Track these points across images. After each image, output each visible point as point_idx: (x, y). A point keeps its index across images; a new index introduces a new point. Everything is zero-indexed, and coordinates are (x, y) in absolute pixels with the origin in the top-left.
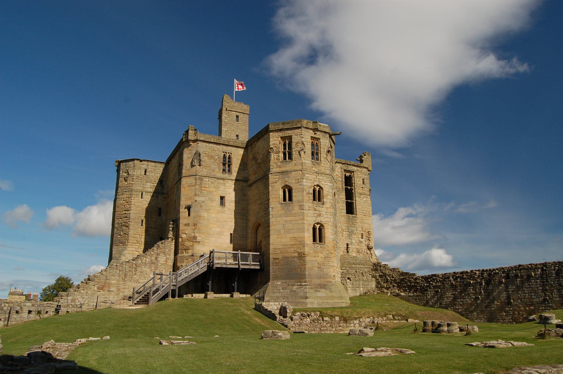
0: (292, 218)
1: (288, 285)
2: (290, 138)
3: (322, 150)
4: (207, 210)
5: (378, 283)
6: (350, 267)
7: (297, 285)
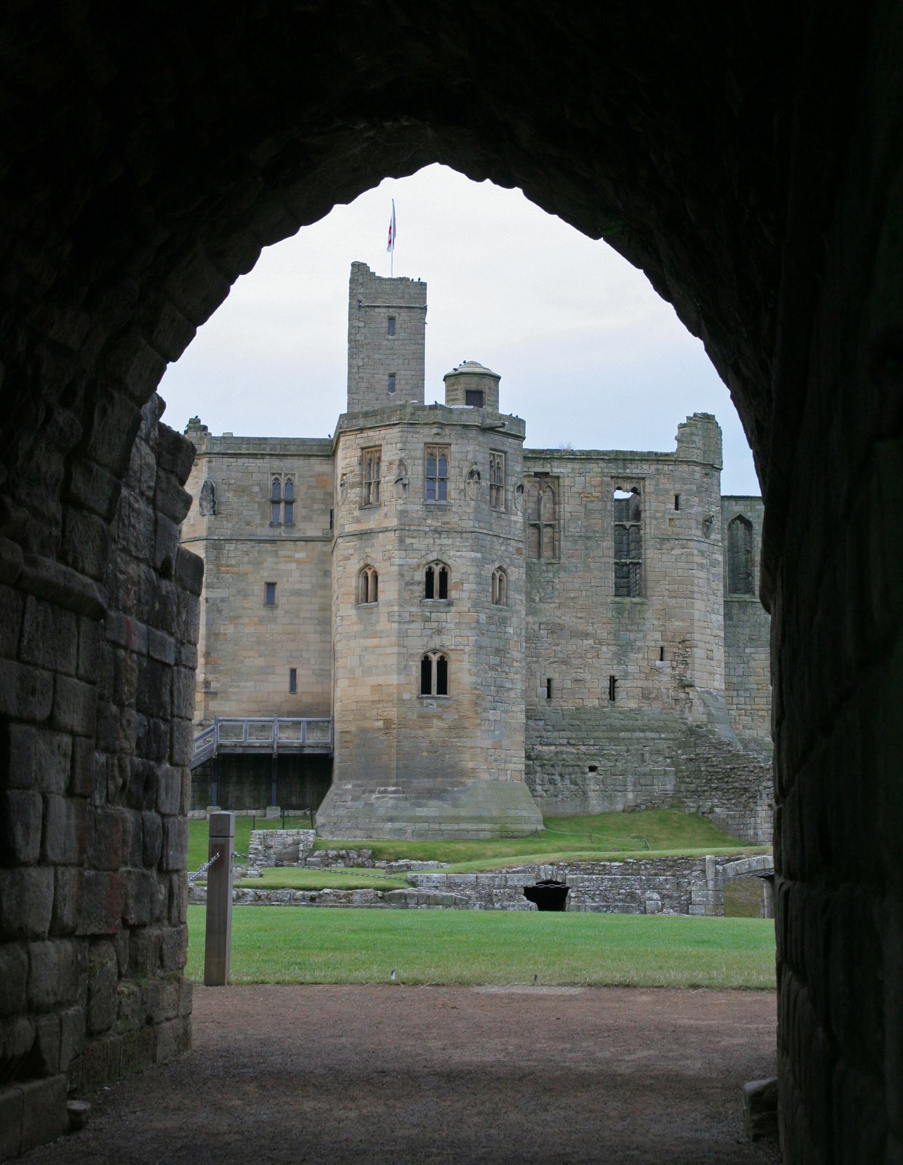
0: (376, 641)
1: (364, 792)
2: (378, 448)
3: (452, 472)
4: (234, 619)
5: (681, 780)
6: (611, 739)
7: (380, 792)
